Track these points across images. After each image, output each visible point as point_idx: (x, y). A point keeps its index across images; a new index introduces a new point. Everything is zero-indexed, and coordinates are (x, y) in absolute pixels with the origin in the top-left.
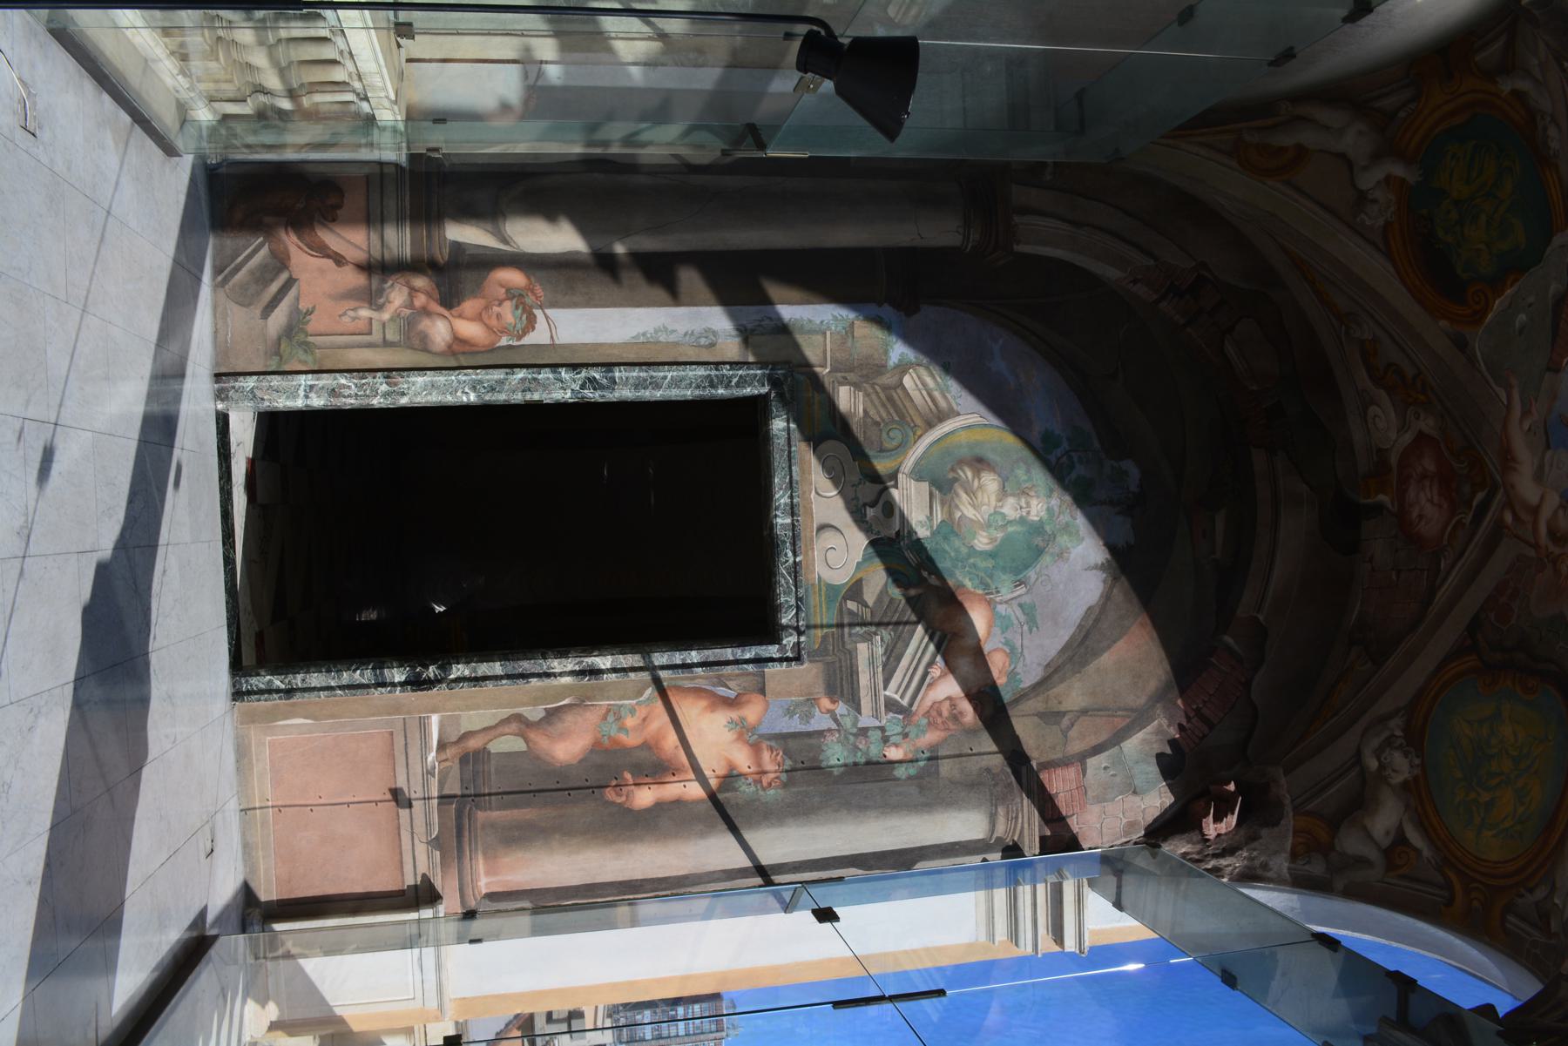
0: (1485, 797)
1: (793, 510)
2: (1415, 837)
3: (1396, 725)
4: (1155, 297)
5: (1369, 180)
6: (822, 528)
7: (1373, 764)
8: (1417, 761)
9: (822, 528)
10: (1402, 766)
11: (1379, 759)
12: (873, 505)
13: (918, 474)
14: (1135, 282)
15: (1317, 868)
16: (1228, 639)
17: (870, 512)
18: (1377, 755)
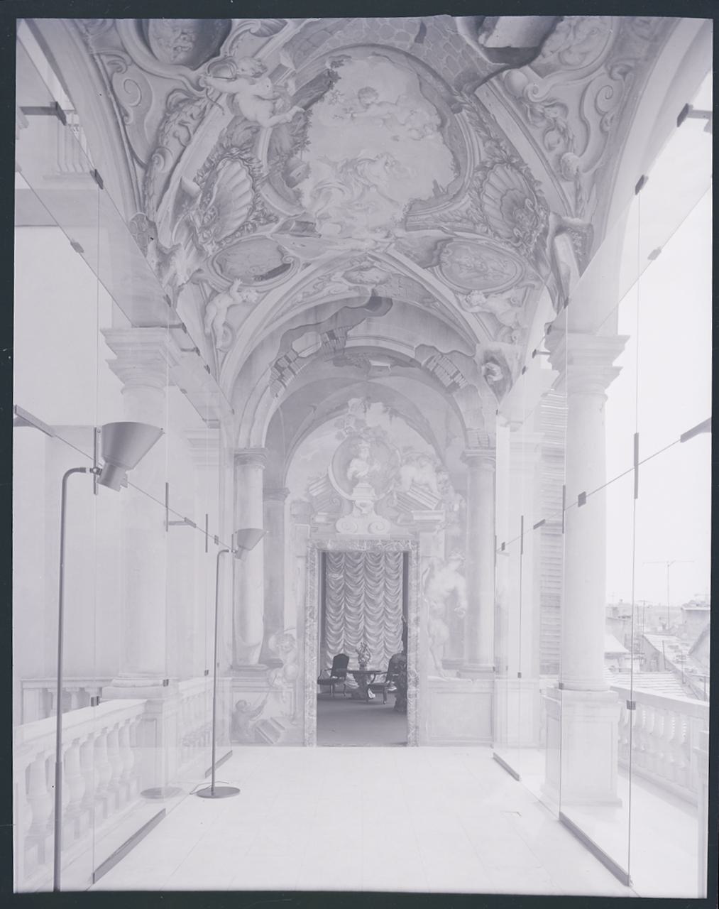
0: (491, 270)
1: (362, 542)
2: (507, 295)
3: (461, 297)
4: (283, 387)
5: (239, 300)
6: (369, 530)
7: (477, 309)
8: (477, 292)
9: (369, 530)
10: (477, 297)
11: (475, 306)
12: (361, 510)
13: (351, 492)
14: (277, 396)
15: (517, 334)
16: (423, 363)
17: (364, 511)
18: (471, 306)
